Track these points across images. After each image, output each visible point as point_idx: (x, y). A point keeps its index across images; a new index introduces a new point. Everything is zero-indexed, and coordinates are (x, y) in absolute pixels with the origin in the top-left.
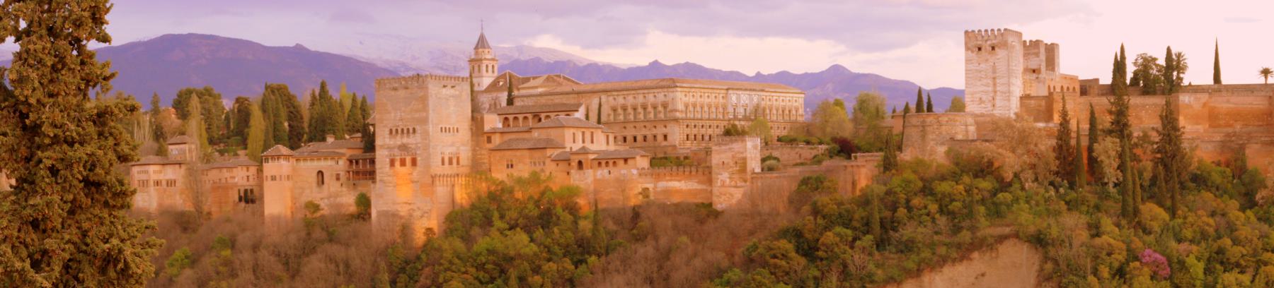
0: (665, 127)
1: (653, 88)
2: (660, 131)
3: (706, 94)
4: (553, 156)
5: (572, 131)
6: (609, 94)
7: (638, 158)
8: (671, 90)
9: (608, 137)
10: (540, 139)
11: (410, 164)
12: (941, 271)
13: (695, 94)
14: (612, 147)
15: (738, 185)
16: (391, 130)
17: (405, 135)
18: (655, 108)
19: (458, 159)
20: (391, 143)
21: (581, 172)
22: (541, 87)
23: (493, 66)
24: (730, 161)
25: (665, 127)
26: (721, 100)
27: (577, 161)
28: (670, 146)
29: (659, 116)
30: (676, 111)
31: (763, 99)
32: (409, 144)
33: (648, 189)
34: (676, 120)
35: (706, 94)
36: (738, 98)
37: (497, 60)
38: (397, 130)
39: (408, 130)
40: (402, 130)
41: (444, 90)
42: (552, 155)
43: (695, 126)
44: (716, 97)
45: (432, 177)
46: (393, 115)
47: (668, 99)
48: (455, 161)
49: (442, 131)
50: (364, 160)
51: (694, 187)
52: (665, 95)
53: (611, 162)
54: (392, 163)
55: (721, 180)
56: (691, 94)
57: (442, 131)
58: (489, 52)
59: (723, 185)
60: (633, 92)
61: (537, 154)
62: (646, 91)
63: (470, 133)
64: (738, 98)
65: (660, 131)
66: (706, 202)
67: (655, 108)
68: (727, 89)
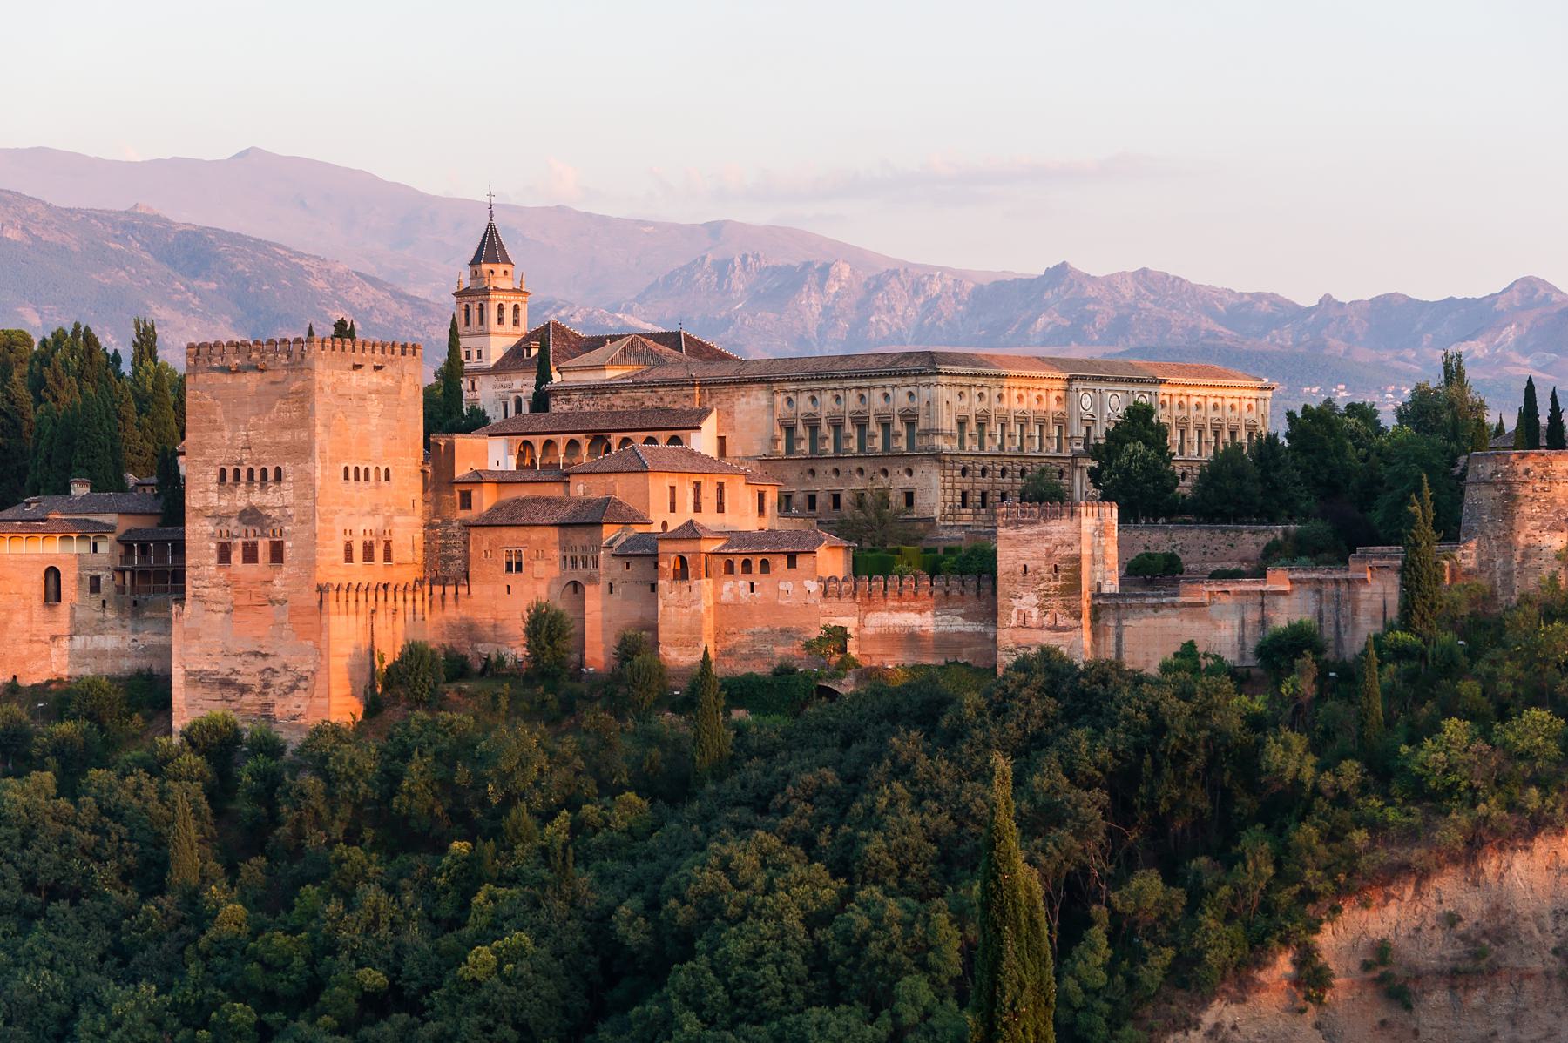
0: (910, 472)
1: (880, 376)
2: (898, 481)
3: (1016, 393)
4: (615, 545)
5: (668, 481)
6: (776, 387)
7: (821, 551)
8: (925, 380)
9: (761, 496)
10: (589, 501)
11: (268, 559)
12: (1527, 849)
13: (985, 391)
14: (771, 521)
15: (1060, 623)
16: (223, 472)
17: (242, 485)
18: (886, 425)
19: (388, 544)
20: (223, 503)
21: (685, 585)
22: (614, 363)
23: (516, 309)
24: (1042, 563)
25: (910, 472)
26: (1054, 407)
27: (673, 557)
28: (919, 520)
29: (894, 444)
30: (937, 433)
31: (1163, 405)
32: (264, 507)
33: (844, 629)
34: (937, 456)
35: (1016, 393)
36: (1099, 404)
37: (527, 294)
38: (237, 472)
39: (264, 472)
40: (251, 472)
41: (355, 375)
42: (613, 541)
43: (984, 472)
44: (1039, 398)
45: (321, 590)
46: (227, 434)
47: (919, 404)
48: (379, 552)
49: (346, 477)
50: (161, 544)
51: (954, 628)
52: (911, 394)
53: (756, 562)
54: (224, 555)
55: (1020, 612)
56: (975, 391)
57: (346, 477)
58: (505, 272)
59: (1024, 625)
60: (832, 385)
61: (580, 538)
62: (865, 383)
63: (419, 483)
64: (1099, 404)
65: (898, 481)
66: (980, 663)
67: (886, 425)
68: (1069, 380)
